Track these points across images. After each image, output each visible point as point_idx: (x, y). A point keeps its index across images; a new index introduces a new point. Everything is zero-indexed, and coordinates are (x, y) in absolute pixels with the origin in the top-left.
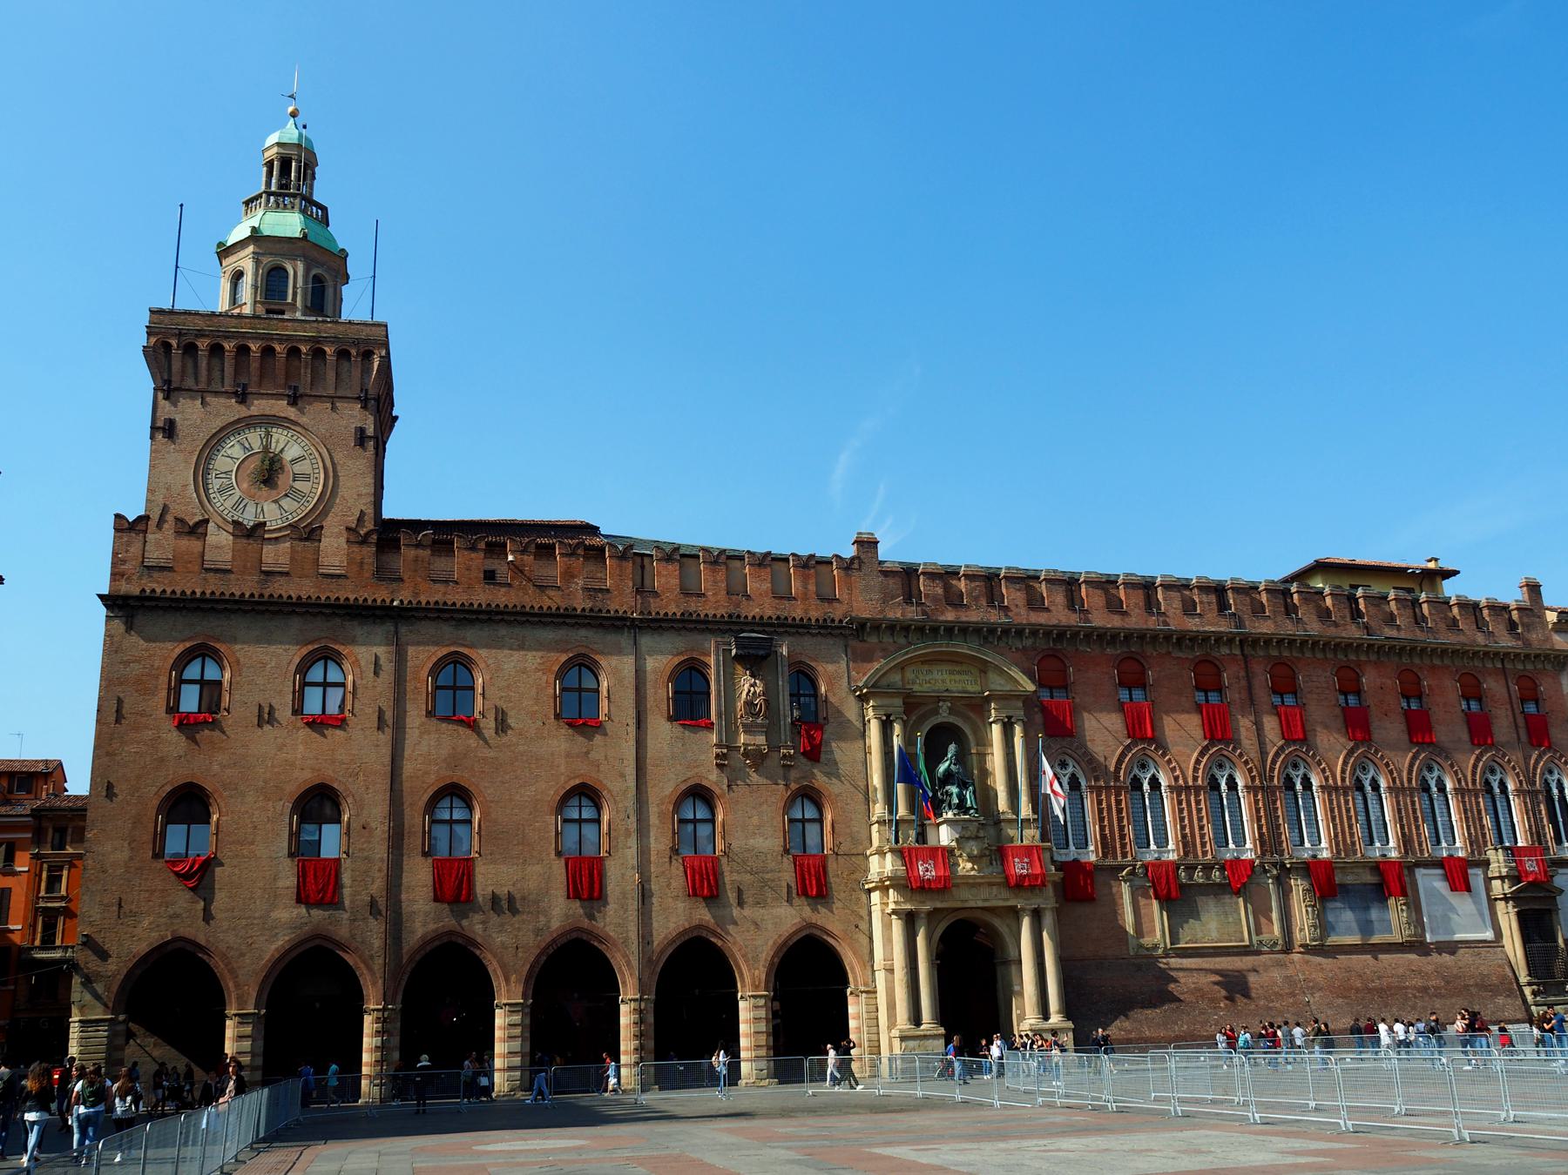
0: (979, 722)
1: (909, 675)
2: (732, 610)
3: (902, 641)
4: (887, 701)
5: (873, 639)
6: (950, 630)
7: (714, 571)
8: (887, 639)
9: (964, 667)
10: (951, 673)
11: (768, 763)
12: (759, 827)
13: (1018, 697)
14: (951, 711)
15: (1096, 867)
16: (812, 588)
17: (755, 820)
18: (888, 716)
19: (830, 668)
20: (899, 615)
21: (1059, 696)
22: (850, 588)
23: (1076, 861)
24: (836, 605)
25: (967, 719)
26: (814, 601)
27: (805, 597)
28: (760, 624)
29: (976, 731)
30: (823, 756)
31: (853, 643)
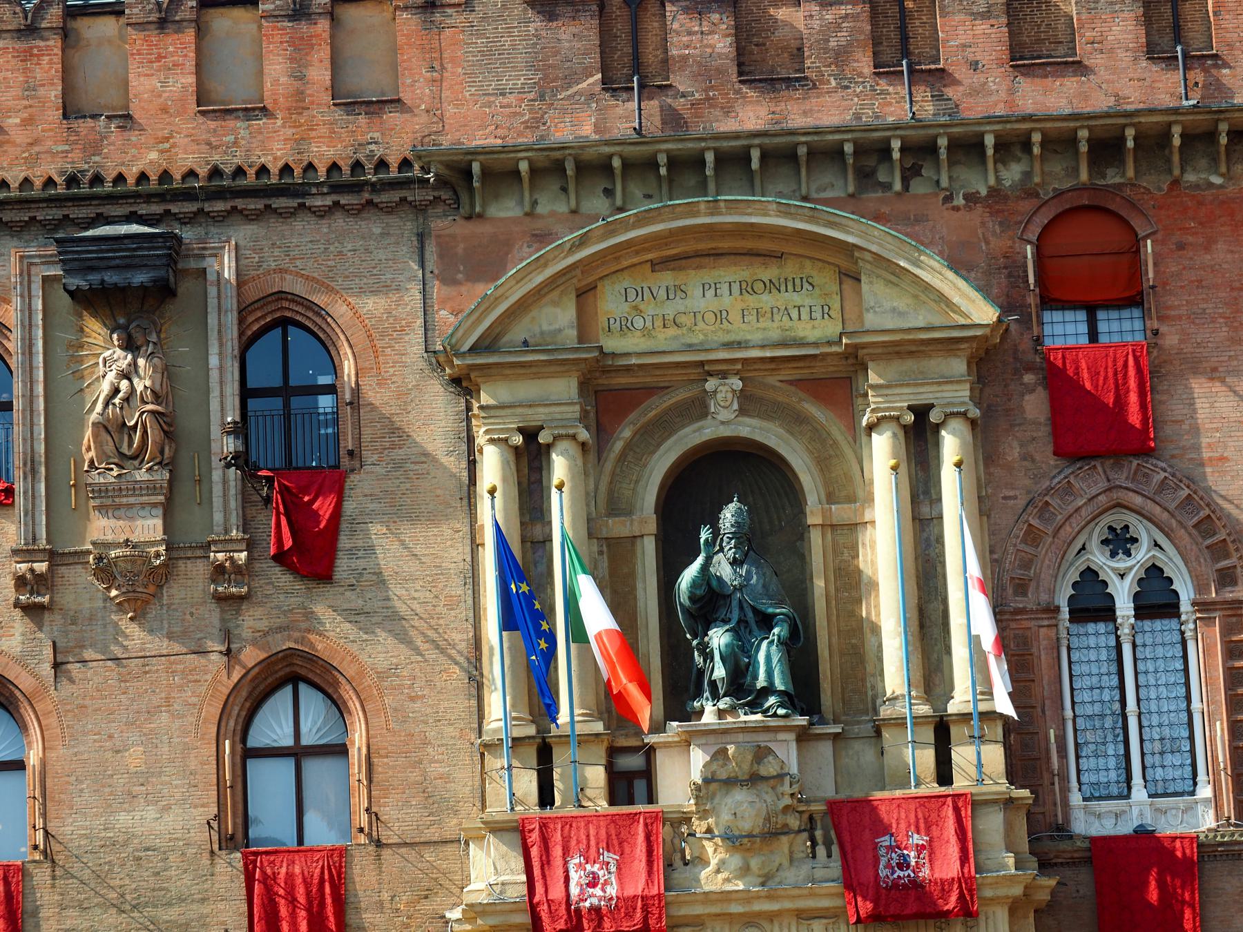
0: (837, 431)
1: (611, 302)
2: (77, 161)
3: (596, 203)
4: (526, 390)
5: (506, 209)
6: (736, 162)
7: (27, 56)
8: (551, 204)
9: (790, 269)
10: (748, 288)
11: (175, 592)
12: (144, 777)
13: (949, 345)
14: (748, 403)
15: (1207, 852)
16: (320, 74)
17: (135, 757)
18: (530, 434)
19: (372, 305)
20: (587, 130)
21: (1120, 328)
22: (437, 66)
23: (1144, 835)
24: (392, 117)
25: (796, 421)
26: (323, 112)
27: (299, 102)
28: (167, 195)
29: (825, 461)
30: (343, 565)
31: (441, 224)
